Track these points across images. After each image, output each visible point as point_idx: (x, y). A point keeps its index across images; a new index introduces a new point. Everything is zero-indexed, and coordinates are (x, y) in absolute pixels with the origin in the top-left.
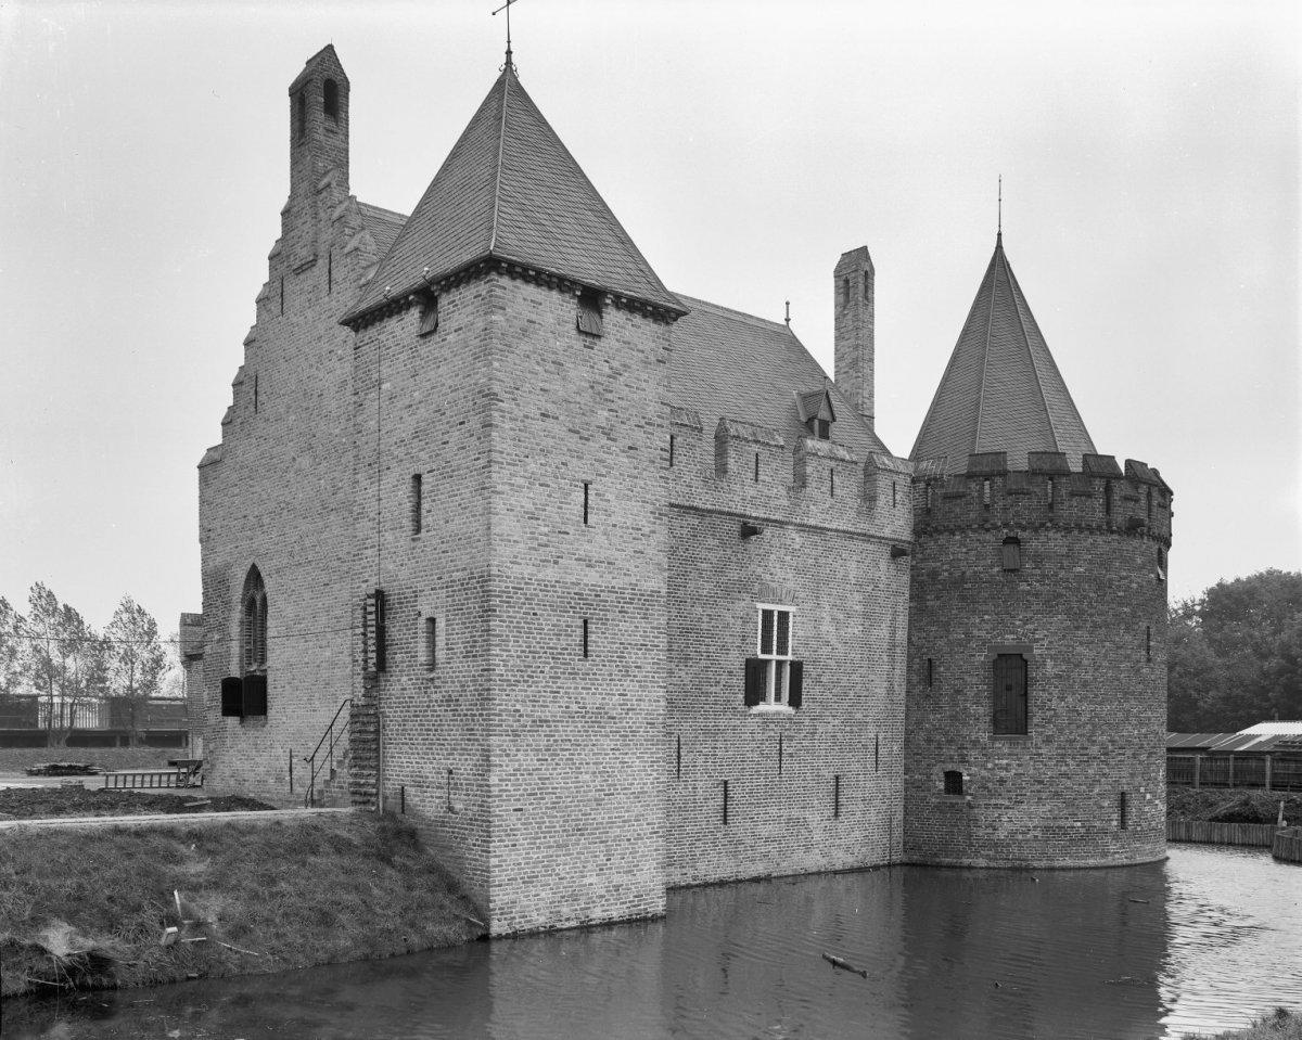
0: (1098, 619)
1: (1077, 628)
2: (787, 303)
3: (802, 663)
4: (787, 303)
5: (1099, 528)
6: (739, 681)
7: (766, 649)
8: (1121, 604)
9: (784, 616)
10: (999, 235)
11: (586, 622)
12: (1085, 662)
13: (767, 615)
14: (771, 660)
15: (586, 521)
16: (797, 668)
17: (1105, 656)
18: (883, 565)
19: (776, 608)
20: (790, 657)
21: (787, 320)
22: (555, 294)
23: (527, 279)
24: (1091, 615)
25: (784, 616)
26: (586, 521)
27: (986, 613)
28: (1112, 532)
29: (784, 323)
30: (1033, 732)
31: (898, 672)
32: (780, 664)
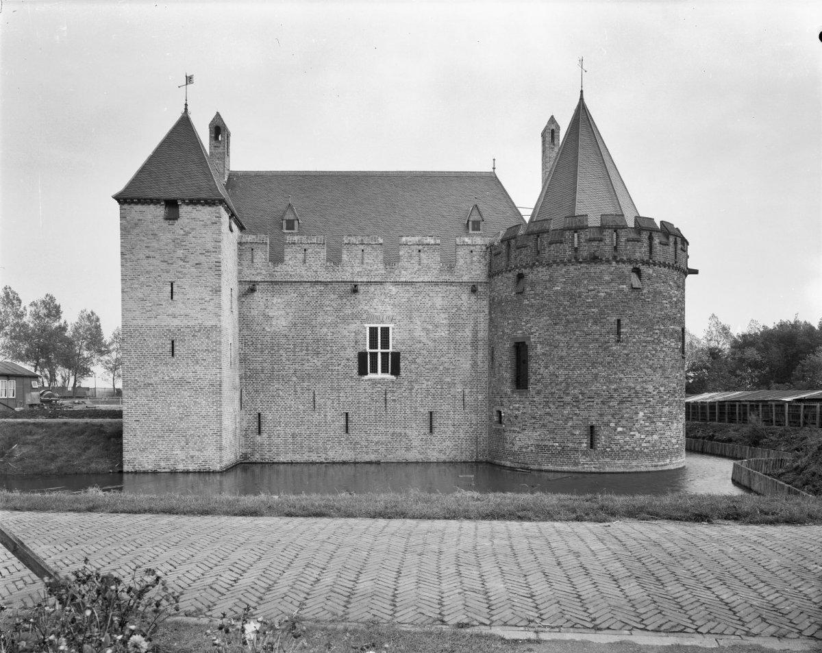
0: (570, 317)
1: (556, 324)
2: (494, 160)
3: (399, 353)
4: (494, 160)
5: (570, 261)
6: (355, 364)
7: (373, 345)
8: (590, 307)
9: (387, 329)
10: (582, 91)
11: (173, 342)
12: (562, 345)
13: (373, 331)
14: (377, 353)
15: (172, 298)
16: (396, 356)
17: (576, 340)
18: (465, 297)
19: (379, 326)
20: (391, 350)
21: (494, 168)
22: (152, 207)
23: (136, 203)
24: (566, 316)
25: (385, 331)
26: (172, 298)
27: (509, 319)
28: (581, 263)
29: (492, 170)
30: (530, 387)
31: (480, 355)
32: (385, 355)
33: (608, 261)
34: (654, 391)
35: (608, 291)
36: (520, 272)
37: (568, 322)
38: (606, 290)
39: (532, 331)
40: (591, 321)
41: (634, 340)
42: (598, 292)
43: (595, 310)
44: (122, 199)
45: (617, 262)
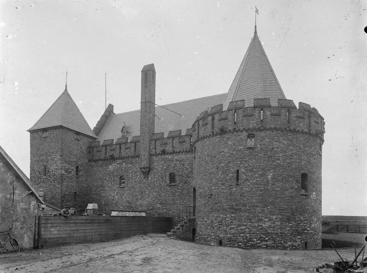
33: (230, 131)
34: (266, 219)
44: (32, 132)
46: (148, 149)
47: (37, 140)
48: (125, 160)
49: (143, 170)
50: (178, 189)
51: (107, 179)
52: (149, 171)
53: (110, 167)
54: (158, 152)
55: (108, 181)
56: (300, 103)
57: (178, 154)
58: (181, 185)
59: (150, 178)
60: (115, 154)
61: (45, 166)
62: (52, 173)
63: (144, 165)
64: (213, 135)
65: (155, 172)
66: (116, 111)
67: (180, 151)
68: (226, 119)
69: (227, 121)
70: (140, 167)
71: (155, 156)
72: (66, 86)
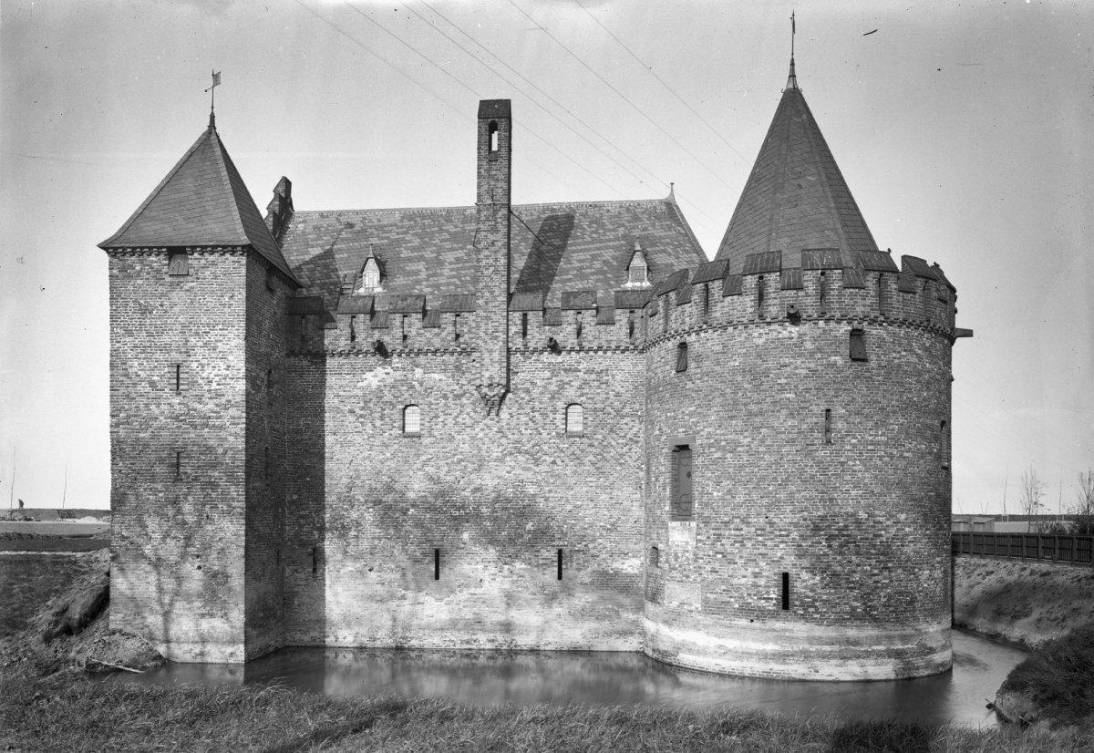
0: (754, 408)
1: (731, 418)
8: (782, 390)
17: (762, 441)
28: (769, 324)
34: (888, 520)
35: (812, 365)
36: (683, 340)
37: (750, 414)
38: (808, 365)
39: (698, 428)
40: (784, 412)
41: (854, 441)
42: (796, 368)
43: (791, 396)
45: (827, 321)
46: (503, 337)
47: (140, 282)
48: (422, 360)
49: (485, 390)
50: (591, 445)
51: (358, 411)
52: (503, 398)
53: (369, 375)
54: (532, 345)
55: (361, 416)
56: (905, 258)
57: (591, 353)
58: (600, 437)
59: (504, 414)
60: (386, 339)
61: (178, 367)
62: (206, 388)
63: (491, 378)
64: (761, 318)
65: (523, 399)
66: (300, 203)
67: (600, 348)
68: (801, 289)
69: (801, 293)
70: (478, 382)
71: (523, 353)
72: (212, 117)
